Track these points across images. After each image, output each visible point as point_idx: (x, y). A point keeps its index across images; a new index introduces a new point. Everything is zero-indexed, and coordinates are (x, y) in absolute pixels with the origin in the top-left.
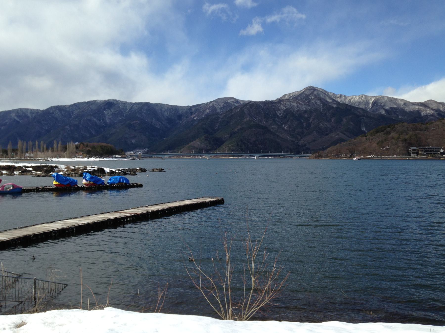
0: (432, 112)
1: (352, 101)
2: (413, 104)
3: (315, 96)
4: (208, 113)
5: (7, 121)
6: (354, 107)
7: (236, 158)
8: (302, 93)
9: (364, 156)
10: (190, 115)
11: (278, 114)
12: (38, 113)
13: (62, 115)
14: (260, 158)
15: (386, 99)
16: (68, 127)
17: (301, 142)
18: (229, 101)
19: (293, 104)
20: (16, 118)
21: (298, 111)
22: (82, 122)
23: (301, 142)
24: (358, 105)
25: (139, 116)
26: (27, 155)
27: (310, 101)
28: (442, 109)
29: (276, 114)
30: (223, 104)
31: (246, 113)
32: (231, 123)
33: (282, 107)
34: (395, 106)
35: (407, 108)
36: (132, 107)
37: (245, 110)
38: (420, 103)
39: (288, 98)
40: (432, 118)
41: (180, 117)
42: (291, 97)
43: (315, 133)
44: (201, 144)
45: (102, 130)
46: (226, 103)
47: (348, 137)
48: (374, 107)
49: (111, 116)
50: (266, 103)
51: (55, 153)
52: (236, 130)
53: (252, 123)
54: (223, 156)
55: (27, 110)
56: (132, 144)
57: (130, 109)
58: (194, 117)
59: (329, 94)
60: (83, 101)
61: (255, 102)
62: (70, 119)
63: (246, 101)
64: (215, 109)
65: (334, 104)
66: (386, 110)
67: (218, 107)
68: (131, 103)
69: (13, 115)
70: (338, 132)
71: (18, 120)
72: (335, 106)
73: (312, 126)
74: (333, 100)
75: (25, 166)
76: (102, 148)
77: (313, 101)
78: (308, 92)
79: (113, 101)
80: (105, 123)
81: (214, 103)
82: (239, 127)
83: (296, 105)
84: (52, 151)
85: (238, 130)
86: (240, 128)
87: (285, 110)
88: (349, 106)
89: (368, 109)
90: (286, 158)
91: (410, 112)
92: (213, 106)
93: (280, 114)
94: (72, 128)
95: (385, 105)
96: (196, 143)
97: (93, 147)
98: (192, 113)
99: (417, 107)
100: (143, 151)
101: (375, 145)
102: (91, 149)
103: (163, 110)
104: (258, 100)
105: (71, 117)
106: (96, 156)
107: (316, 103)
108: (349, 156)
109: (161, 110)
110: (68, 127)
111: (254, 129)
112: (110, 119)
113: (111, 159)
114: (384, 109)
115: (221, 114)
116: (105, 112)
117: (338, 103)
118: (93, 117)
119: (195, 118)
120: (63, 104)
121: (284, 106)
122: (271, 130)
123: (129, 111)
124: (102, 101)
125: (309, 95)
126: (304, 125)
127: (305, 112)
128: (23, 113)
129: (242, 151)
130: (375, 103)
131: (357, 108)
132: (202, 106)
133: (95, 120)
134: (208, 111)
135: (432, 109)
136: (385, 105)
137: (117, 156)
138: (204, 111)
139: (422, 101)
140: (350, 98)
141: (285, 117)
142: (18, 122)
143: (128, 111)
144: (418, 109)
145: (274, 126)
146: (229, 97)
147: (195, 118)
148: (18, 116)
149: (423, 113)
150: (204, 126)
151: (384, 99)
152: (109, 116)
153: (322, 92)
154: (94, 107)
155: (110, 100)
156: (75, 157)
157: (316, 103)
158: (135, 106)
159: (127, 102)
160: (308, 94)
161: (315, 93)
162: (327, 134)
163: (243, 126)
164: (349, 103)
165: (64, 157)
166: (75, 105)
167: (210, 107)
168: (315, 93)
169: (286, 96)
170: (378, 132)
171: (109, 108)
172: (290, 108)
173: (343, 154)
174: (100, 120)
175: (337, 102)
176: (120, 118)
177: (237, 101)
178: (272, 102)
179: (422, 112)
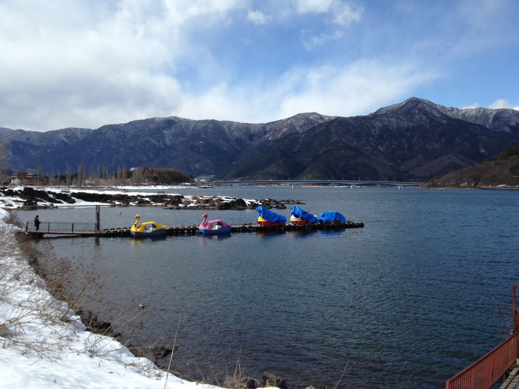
1: (466, 115)
3: (420, 110)
4: (285, 132)
5: (54, 142)
6: (469, 124)
7: (321, 187)
8: (403, 106)
10: (263, 134)
11: (373, 133)
12: (88, 133)
13: (116, 136)
15: (511, 113)
16: (122, 149)
17: (402, 168)
18: (311, 117)
19: (392, 120)
20: (64, 139)
21: (397, 129)
24: (475, 121)
25: (203, 136)
26: (87, 182)
27: (413, 116)
30: (303, 121)
31: (333, 131)
32: (315, 144)
33: (379, 124)
36: (195, 126)
37: (332, 128)
39: (385, 112)
41: (251, 137)
42: (388, 111)
43: (420, 156)
44: (278, 169)
45: (161, 153)
47: (463, 161)
49: (171, 137)
50: (358, 119)
51: (119, 180)
52: (321, 152)
53: (341, 144)
54: (305, 184)
55: (76, 129)
56: (196, 169)
57: (193, 128)
58: (268, 137)
59: (437, 107)
61: (344, 118)
62: (125, 140)
63: (332, 117)
65: (444, 119)
66: (511, 127)
68: (194, 121)
69: (61, 136)
71: (67, 141)
72: (445, 122)
73: (416, 147)
74: (443, 114)
75: (139, 196)
76: (170, 174)
77: (417, 117)
78: (410, 106)
79: (173, 119)
80: (165, 145)
81: (293, 120)
82: (324, 149)
84: (116, 178)
87: (382, 127)
88: (464, 122)
89: (488, 126)
90: (384, 187)
92: (292, 123)
94: (127, 151)
95: (509, 121)
96: (273, 169)
97: (159, 173)
98: (265, 132)
100: (208, 177)
101: (507, 172)
102: (157, 176)
105: (126, 138)
106: (163, 183)
109: (229, 129)
110: (122, 149)
111: (343, 152)
112: (170, 140)
113: (180, 187)
114: (508, 125)
115: (302, 133)
116: (165, 132)
117: (449, 118)
120: (118, 123)
121: (381, 123)
122: (365, 152)
123: (192, 130)
124: (162, 118)
125: (412, 109)
126: (406, 147)
128: (72, 133)
131: (473, 124)
132: (278, 123)
133: (153, 141)
134: (285, 130)
137: (186, 184)
138: (280, 130)
140: (464, 112)
142: (66, 144)
143: (190, 130)
145: (368, 148)
146: (311, 112)
147: (270, 139)
148: (67, 137)
150: (281, 148)
152: (169, 136)
153: (427, 104)
154: (152, 126)
155: (170, 117)
156: (141, 185)
158: (199, 124)
159: (190, 120)
160: (410, 107)
161: (420, 106)
162: (436, 158)
164: (463, 118)
165: (129, 185)
166: (130, 123)
168: (420, 106)
170: (511, 155)
171: (169, 128)
172: (388, 125)
177: (321, 117)
178: (364, 118)
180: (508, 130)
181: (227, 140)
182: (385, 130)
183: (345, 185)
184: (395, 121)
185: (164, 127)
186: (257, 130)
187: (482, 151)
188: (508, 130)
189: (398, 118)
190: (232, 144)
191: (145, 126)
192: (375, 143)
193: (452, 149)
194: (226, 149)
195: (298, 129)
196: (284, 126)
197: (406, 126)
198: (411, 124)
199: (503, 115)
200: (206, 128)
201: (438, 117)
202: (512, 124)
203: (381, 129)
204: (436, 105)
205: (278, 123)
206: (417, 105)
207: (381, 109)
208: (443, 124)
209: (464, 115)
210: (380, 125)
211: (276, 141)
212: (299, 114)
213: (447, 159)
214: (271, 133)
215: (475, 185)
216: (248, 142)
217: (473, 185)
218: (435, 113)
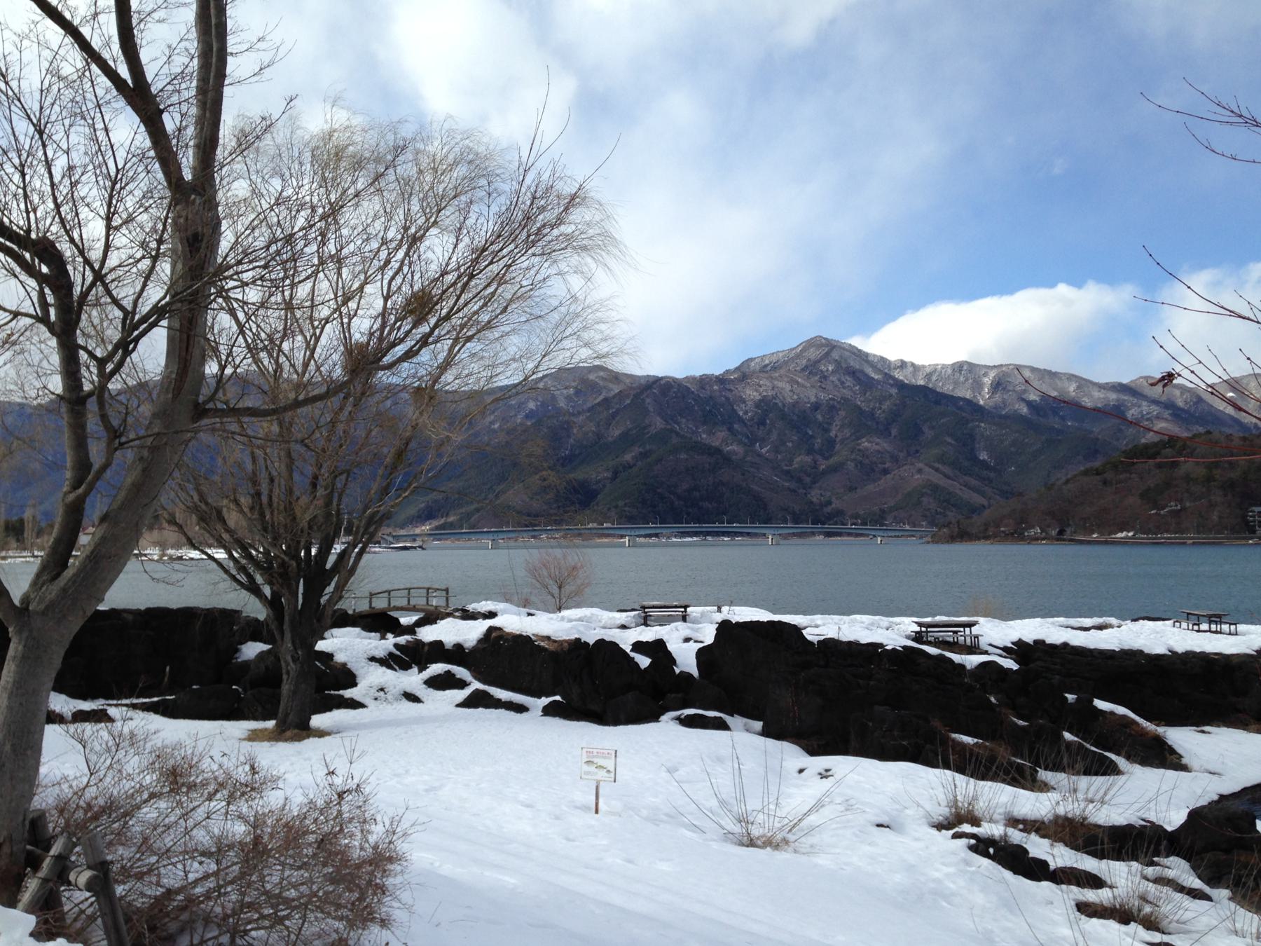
2: (1101, 387)
3: (837, 363)
4: (531, 411)
8: (798, 356)
9: (1101, 534)
11: (741, 413)
14: (709, 538)
18: (592, 377)
19: (780, 384)
28: (1180, 403)
29: (734, 411)
33: (751, 394)
34: (1054, 394)
35: (1085, 399)
37: (648, 400)
38: (1121, 385)
42: (766, 366)
46: (584, 381)
47: (949, 478)
50: (704, 381)
53: (675, 440)
58: (492, 423)
64: (554, 398)
66: (1030, 404)
70: (921, 465)
78: (813, 354)
83: (788, 387)
85: (633, 457)
86: (641, 453)
89: (981, 402)
93: (746, 413)
96: (516, 496)
99: (1113, 396)
104: (679, 374)
107: (842, 383)
108: (1054, 533)
111: (683, 456)
114: (1023, 400)
117: (901, 386)
119: (496, 426)
125: (819, 361)
127: (816, 407)
130: (997, 385)
140: (928, 370)
141: (762, 423)
149: (1131, 414)
157: (842, 383)
160: (813, 357)
161: (835, 355)
162: (886, 472)
163: (648, 447)
168: (835, 355)
173: (1033, 527)
178: (721, 380)
180: (1024, 410)
183: (696, 534)
187: (983, 456)
189: (793, 382)
193: (917, 451)
195: (562, 404)
203: (757, 405)
204: (867, 355)
207: (751, 360)
209: (928, 376)
210: (756, 396)
213: (917, 474)
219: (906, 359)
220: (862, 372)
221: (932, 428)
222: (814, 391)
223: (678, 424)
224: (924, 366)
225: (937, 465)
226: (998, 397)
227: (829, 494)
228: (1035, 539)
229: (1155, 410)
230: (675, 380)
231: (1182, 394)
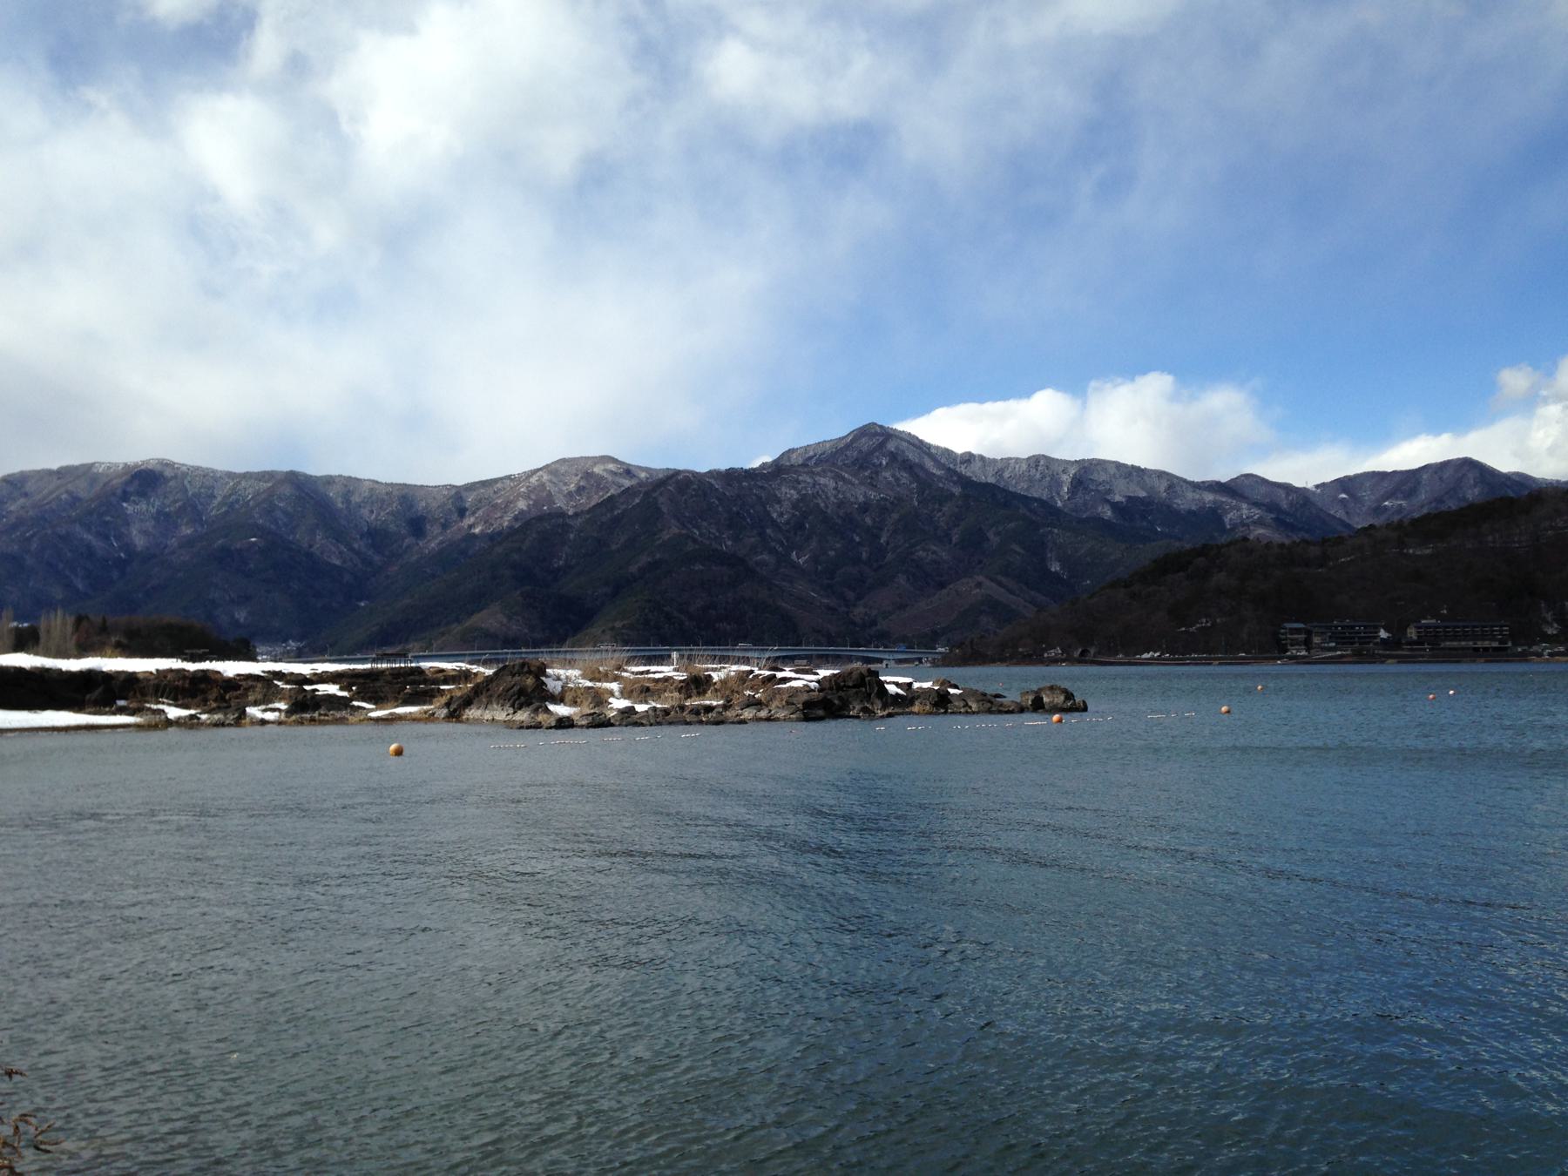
0: (1257, 513)
1: (1006, 475)
3: (893, 457)
4: (522, 512)
6: (1015, 496)
8: (848, 446)
9: (1126, 654)
10: (455, 517)
11: (775, 515)
15: (1112, 471)
17: (859, 612)
18: (597, 470)
19: (822, 481)
21: (841, 504)
22: (34, 546)
23: (859, 612)
27: (877, 473)
28: (1284, 505)
29: (768, 514)
31: (665, 509)
32: (614, 547)
33: (789, 493)
34: (1143, 494)
36: (234, 491)
37: (661, 500)
38: (1218, 483)
40: (1261, 531)
41: (417, 525)
42: (811, 458)
43: (901, 579)
44: (510, 619)
45: (115, 574)
46: (588, 475)
47: (1011, 592)
48: (1079, 499)
49: (150, 525)
52: (633, 569)
53: (690, 547)
56: (236, 624)
57: (225, 497)
58: (471, 527)
60: (39, 467)
64: (550, 498)
66: (1115, 506)
67: (560, 491)
68: (231, 475)
70: (981, 578)
72: (957, 490)
73: (890, 556)
77: (887, 474)
79: (159, 468)
80: (128, 547)
81: (546, 477)
82: (644, 559)
89: (1059, 504)
91: (1190, 512)
95: (1110, 491)
98: (462, 512)
99: (1209, 497)
103: (356, 499)
104: (702, 468)
107: (897, 480)
109: (347, 501)
111: (698, 567)
112: (145, 533)
114: (1108, 501)
115: (576, 515)
117: (966, 482)
118: (78, 528)
124: (117, 465)
125: (871, 453)
126: (864, 555)
127: (865, 508)
129: (663, 641)
132: (499, 485)
134: (522, 505)
135: (1256, 504)
136: (1110, 491)
139: (1224, 477)
140: (999, 466)
141: (800, 526)
143: (216, 502)
144: (1215, 502)
149: (1230, 518)
150: (516, 557)
151: (1105, 470)
154: (82, 489)
158: (243, 484)
159: (214, 471)
160: (865, 449)
161: (891, 446)
162: (942, 585)
163: (658, 556)
167: (531, 490)
168: (891, 446)
169: (794, 456)
171: (143, 494)
172: (814, 496)
174: (107, 538)
175: (960, 476)
176: (187, 531)
177: (628, 471)
178: (750, 474)
179: (1226, 512)
181: (339, 536)
182: (806, 509)
184: (832, 484)
185: (125, 492)
186: (434, 505)
187: (1055, 567)
188: (1109, 513)
189: (838, 477)
190: (356, 546)
191: (58, 488)
192: (782, 544)
194: (338, 562)
195: (560, 503)
196: (519, 495)
197: (861, 499)
198: (872, 494)
199: (1095, 476)
200: (271, 492)
201: (940, 478)
202: (1118, 498)
203: (795, 506)
204: (929, 446)
205: (499, 485)
206: (882, 445)
208: (953, 495)
209: (999, 473)
210: (794, 494)
211: (494, 538)
212: (564, 461)
214: (480, 513)
215: (1083, 653)
216: (407, 541)
217: (1077, 654)
218: (929, 464)
219: (975, 452)
220: (922, 467)
221: (998, 534)
222: (863, 488)
223: (698, 528)
224: (995, 461)
225: (1000, 578)
226: (1079, 499)
227: (874, 612)
228: (1055, 661)
229: (1257, 513)
230: (695, 474)
231: (1288, 495)
